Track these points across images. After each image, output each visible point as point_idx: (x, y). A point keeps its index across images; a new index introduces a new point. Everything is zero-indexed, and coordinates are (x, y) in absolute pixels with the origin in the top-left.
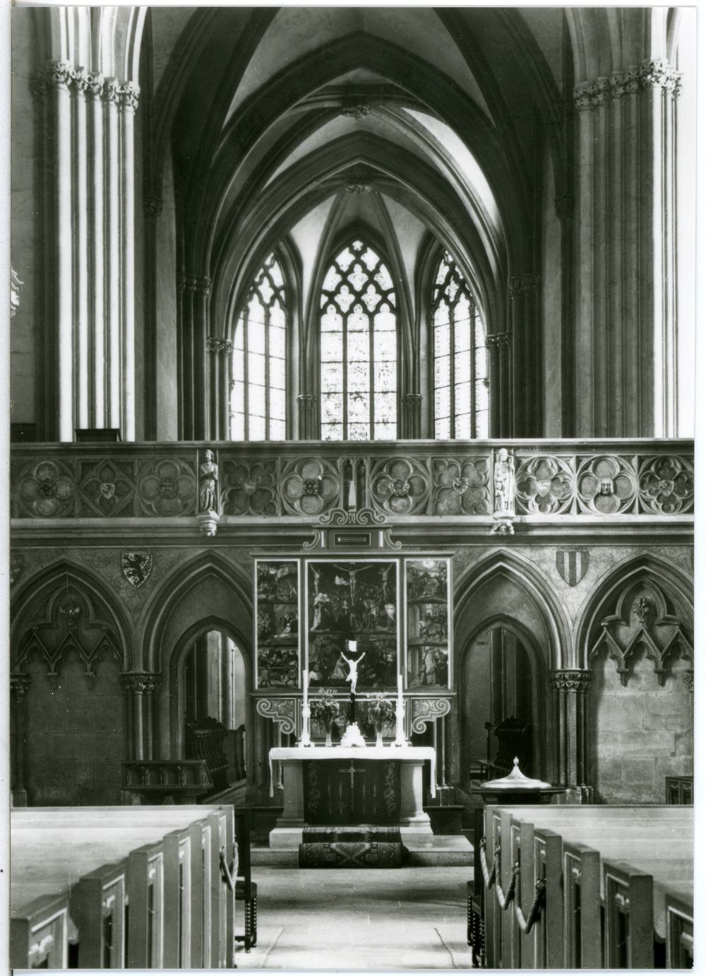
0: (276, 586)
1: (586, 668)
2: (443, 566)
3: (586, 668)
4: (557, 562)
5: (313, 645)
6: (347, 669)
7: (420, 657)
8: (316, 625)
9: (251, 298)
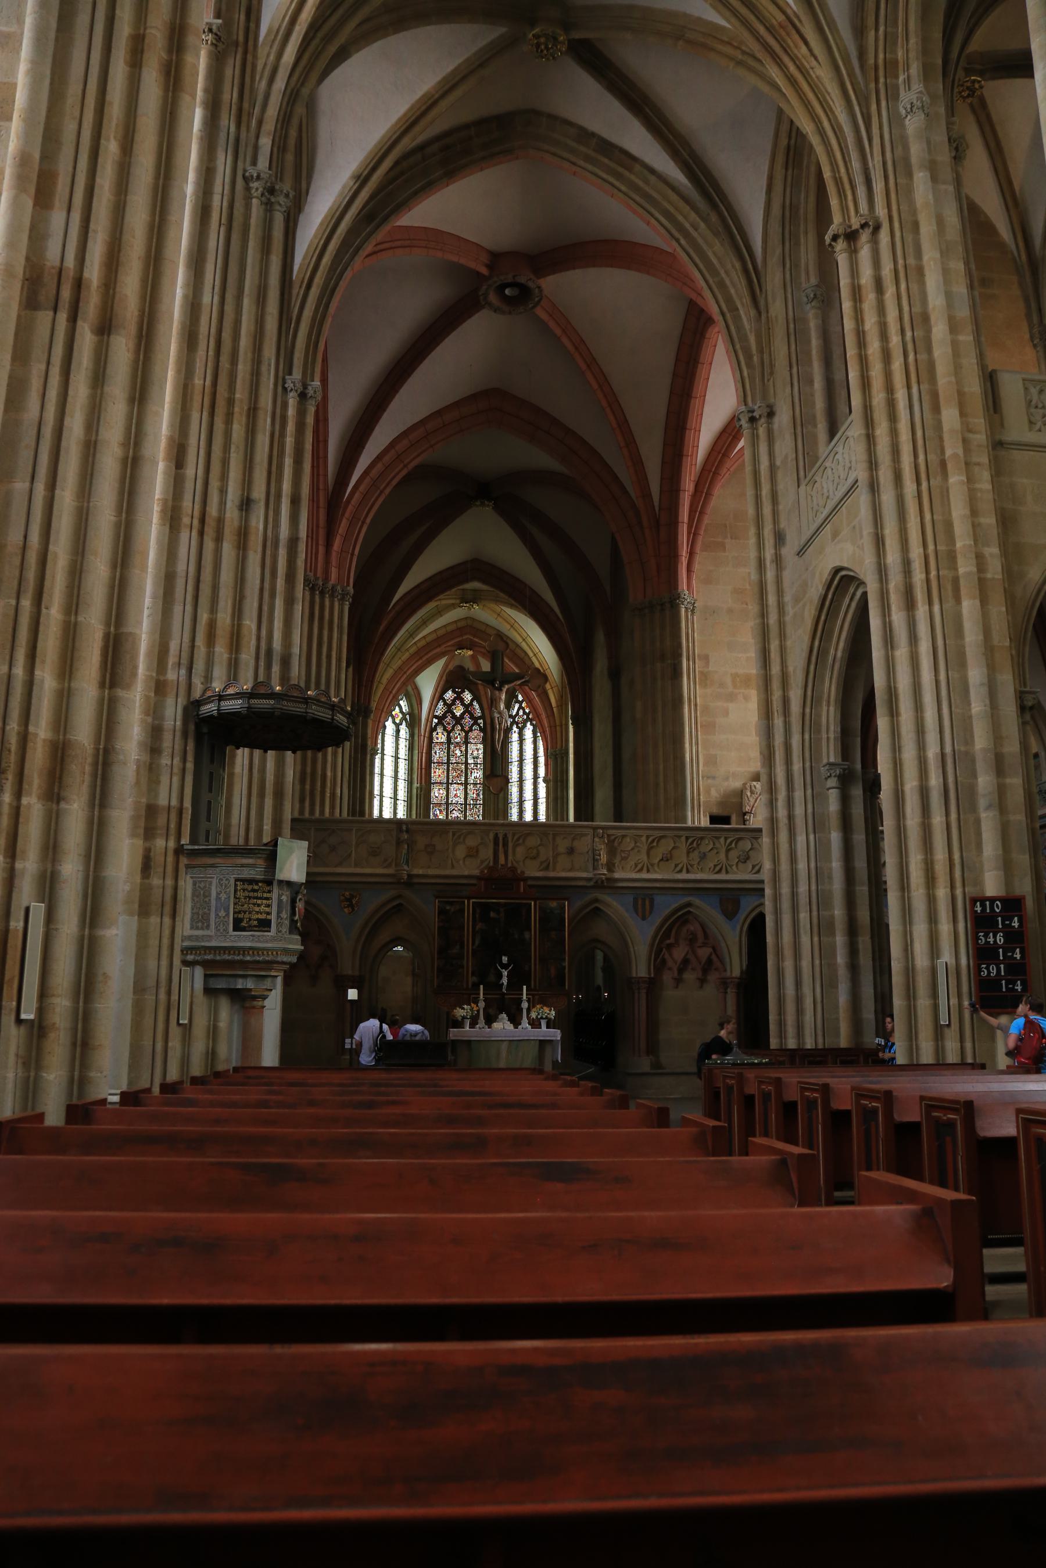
1: (652, 975)
3: (652, 975)
6: (501, 976)
9: (387, 721)
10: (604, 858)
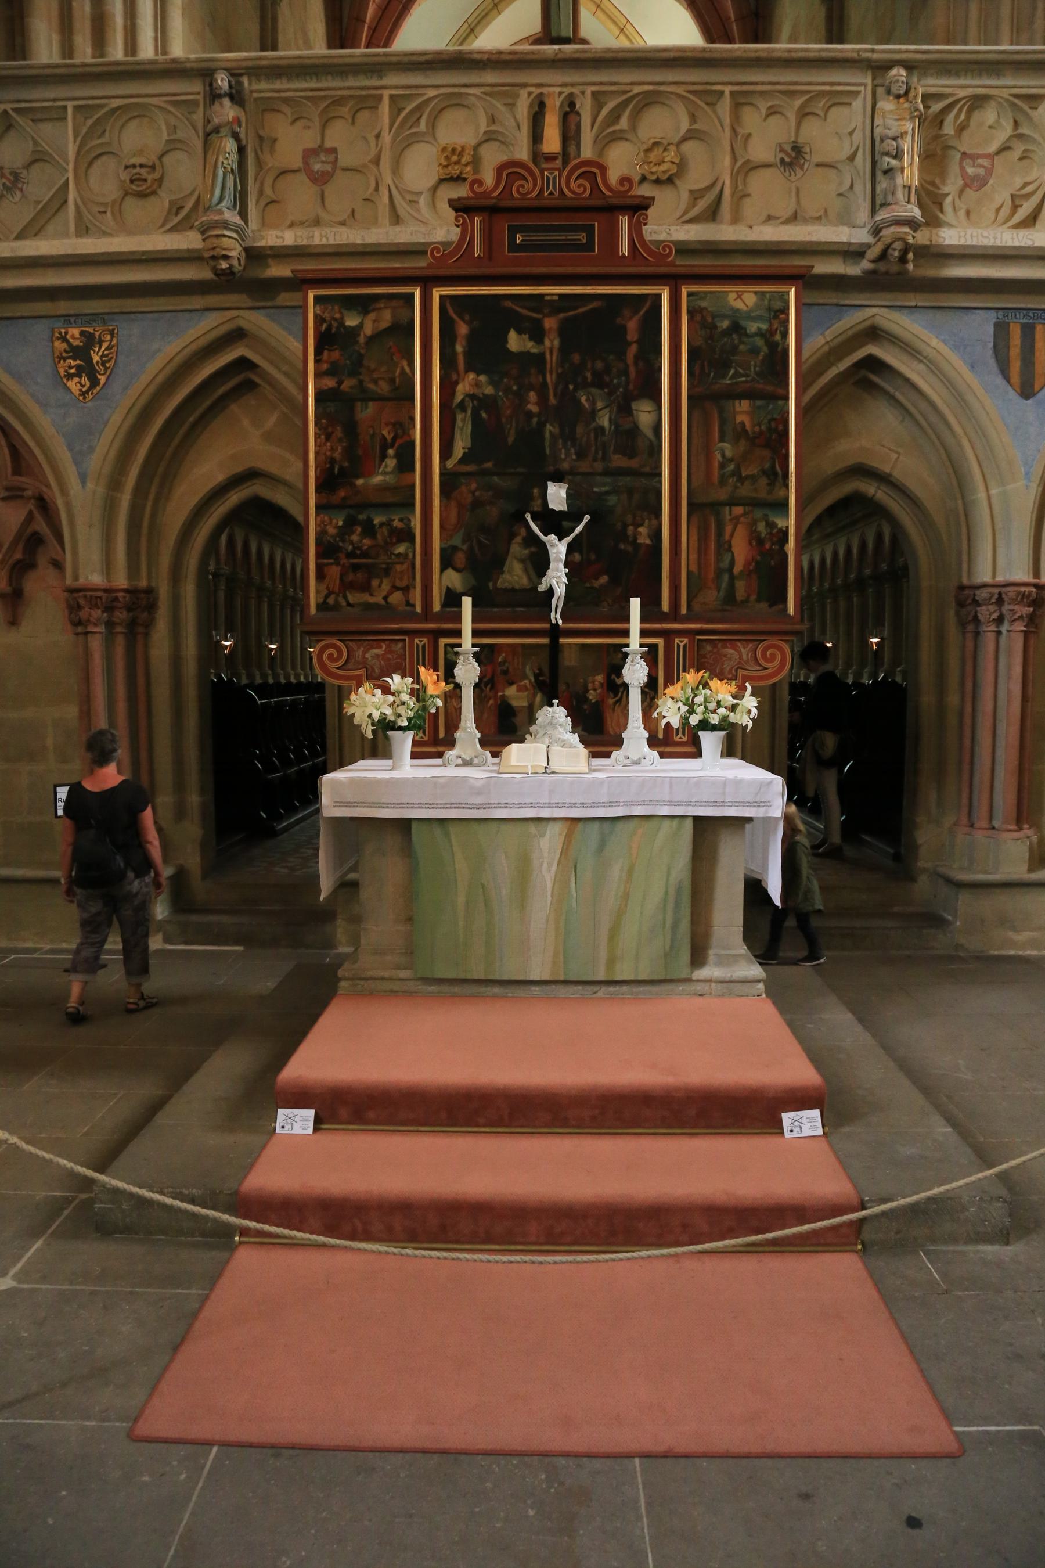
0: (361, 357)
2: (778, 305)
4: (995, 346)
5: (453, 503)
7: (720, 533)
10: (910, 172)
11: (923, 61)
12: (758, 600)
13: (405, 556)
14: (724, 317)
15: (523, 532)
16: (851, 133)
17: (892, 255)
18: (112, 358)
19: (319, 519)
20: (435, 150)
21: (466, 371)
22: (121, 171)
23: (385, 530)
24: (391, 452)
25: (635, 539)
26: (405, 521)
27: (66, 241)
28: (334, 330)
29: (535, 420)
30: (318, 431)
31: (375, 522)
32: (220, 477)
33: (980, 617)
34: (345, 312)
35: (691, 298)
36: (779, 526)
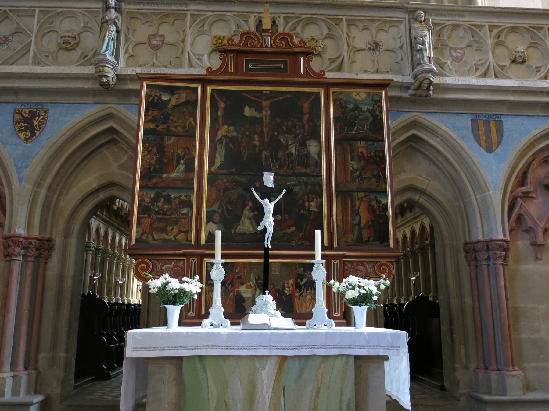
0: (169, 115)
2: (377, 98)
4: (472, 130)
6: (260, 213)
7: (353, 206)
8: (218, 163)
11: (430, 9)
12: (374, 241)
13: (187, 215)
14: (351, 103)
15: (251, 204)
16: (400, 38)
17: (424, 86)
18: (44, 123)
19: (141, 193)
20: (210, 38)
21: (223, 125)
22: (59, 38)
23: (177, 201)
24: (182, 161)
25: (309, 208)
26: (188, 196)
27: (26, 67)
28: (155, 101)
29: (257, 149)
30: (143, 149)
31: (172, 196)
32: (95, 185)
33: (478, 258)
34: (162, 93)
35: (334, 94)
36: (383, 203)
